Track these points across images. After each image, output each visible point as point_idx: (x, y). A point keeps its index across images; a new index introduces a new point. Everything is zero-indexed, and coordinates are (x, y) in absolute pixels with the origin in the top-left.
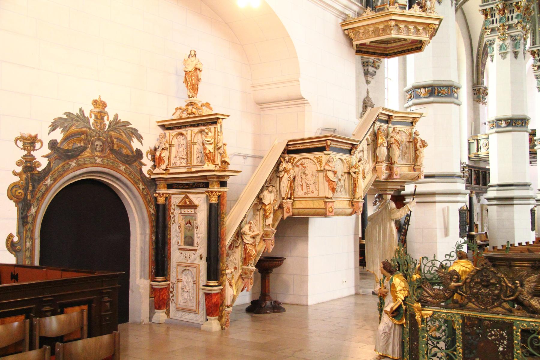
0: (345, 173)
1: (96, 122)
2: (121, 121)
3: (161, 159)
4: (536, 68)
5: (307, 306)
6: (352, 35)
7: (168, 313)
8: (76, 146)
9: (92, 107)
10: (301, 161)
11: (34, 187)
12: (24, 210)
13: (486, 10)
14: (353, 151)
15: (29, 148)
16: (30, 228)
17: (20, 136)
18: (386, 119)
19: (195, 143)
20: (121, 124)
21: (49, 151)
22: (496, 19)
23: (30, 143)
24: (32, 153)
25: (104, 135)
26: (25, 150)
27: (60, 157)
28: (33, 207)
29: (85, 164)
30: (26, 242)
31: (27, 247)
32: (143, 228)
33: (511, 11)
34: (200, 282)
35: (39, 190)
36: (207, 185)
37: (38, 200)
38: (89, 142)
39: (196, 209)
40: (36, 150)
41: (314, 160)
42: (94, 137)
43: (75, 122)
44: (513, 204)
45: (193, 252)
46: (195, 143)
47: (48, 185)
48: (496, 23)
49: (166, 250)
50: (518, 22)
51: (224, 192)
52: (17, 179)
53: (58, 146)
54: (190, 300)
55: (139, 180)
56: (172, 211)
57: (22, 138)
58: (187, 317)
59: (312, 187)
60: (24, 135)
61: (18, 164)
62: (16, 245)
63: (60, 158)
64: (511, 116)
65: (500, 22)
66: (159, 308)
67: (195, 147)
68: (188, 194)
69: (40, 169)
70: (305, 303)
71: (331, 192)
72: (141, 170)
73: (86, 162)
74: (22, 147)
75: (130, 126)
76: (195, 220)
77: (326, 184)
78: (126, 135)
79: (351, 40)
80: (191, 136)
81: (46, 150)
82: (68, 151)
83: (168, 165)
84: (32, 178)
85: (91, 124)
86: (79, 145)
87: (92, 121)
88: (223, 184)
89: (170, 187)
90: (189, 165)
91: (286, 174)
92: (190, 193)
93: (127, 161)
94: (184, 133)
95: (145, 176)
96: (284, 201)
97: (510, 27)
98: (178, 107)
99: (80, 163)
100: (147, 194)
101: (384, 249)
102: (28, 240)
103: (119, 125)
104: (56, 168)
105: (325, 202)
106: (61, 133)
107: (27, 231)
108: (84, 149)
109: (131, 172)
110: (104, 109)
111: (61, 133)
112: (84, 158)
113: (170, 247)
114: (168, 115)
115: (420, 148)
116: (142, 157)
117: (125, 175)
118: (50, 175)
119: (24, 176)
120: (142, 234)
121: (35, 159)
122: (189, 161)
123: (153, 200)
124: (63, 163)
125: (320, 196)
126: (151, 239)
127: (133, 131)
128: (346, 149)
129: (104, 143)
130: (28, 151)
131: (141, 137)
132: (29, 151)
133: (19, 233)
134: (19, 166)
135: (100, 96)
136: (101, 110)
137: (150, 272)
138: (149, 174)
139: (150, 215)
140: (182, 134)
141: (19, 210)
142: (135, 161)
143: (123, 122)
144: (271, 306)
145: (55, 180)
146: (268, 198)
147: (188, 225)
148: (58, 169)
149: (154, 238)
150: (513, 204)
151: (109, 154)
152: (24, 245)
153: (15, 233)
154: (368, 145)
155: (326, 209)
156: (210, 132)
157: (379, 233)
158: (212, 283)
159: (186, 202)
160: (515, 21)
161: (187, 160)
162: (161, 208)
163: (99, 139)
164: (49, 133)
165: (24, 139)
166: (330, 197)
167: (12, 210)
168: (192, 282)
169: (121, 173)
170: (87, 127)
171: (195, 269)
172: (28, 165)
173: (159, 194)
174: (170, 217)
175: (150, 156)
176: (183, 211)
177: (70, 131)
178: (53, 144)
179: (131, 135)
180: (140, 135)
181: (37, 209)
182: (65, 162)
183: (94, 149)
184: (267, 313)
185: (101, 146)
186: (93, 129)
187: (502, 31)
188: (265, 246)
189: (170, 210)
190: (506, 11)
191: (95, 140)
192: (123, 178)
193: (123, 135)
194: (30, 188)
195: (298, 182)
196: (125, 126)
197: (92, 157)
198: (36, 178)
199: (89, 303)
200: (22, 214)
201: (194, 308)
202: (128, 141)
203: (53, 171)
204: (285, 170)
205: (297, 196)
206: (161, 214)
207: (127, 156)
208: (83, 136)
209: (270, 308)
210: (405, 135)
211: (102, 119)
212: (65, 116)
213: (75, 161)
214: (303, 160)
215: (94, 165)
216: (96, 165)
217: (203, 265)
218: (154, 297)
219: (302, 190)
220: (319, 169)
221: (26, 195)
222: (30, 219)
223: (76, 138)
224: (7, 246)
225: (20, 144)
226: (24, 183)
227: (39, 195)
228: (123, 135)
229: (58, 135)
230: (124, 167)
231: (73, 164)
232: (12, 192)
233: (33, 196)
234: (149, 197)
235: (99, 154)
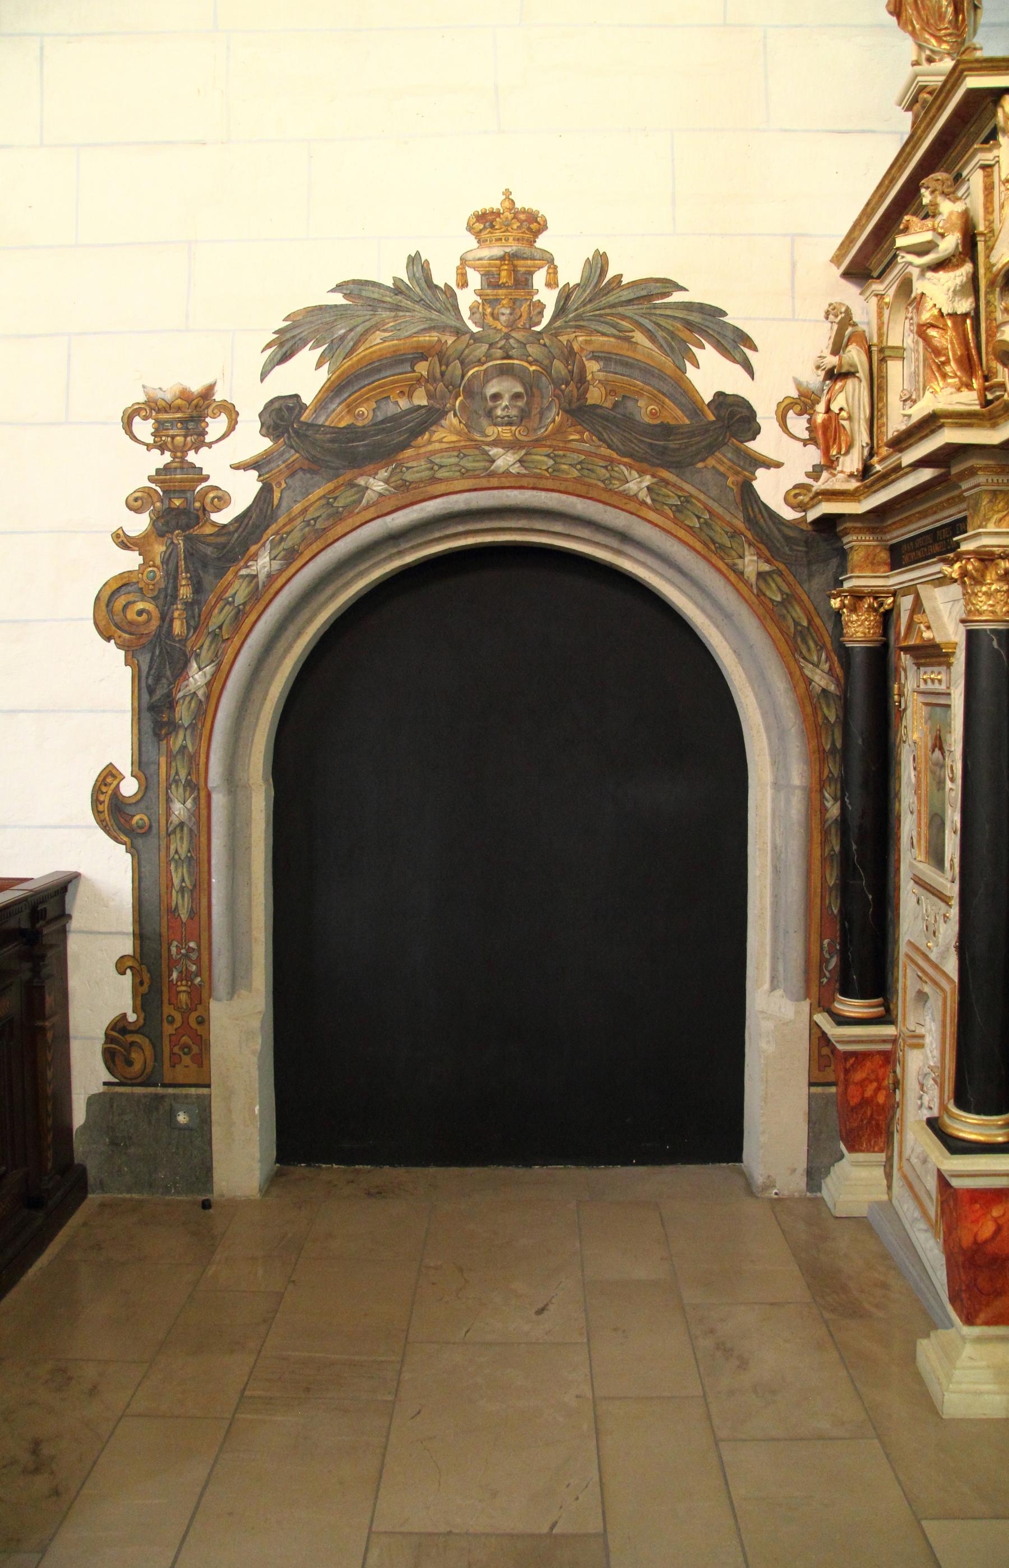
2: (625, 281)
8: (390, 410)
9: (471, 242)
11: (198, 588)
12: (158, 679)
15: (179, 440)
16: (184, 748)
17: (142, 398)
20: (626, 295)
21: (266, 444)
23: (182, 421)
24: (191, 457)
25: (533, 350)
26: (162, 448)
27: (314, 460)
28: (195, 665)
29: (434, 480)
30: (169, 800)
31: (175, 820)
35: (220, 598)
37: (215, 636)
40: (210, 445)
42: (480, 362)
43: (385, 314)
47: (262, 577)
52: (131, 561)
55: (735, 534)
57: (151, 407)
60: (160, 395)
61: (136, 504)
62: (130, 810)
69: (222, 517)
72: (747, 492)
73: (441, 474)
74: (150, 440)
75: (677, 297)
78: (652, 337)
81: (252, 440)
82: (351, 433)
84: (190, 554)
85: (465, 313)
86: (404, 404)
87: (466, 299)
93: (664, 451)
99: (409, 476)
100: (788, 600)
102: (177, 793)
103: (612, 298)
104: (297, 508)
106: (319, 365)
107: (171, 757)
108: (429, 418)
109: (688, 499)
110: (531, 243)
111: (319, 365)
112: (429, 457)
116: (754, 431)
118: (269, 535)
119: (159, 549)
121: (207, 478)
124: (331, 486)
126: (815, 808)
127: (695, 318)
129: (531, 387)
130: (174, 452)
132: (179, 452)
133: (141, 765)
134: (137, 510)
135: (507, 193)
136: (512, 247)
137: (812, 967)
141: (137, 678)
142: (711, 449)
143: (634, 284)
145: (291, 555)
148: (304, 511)
151: (559, 431)
152: (162, 810)
153: (125, 766)
163: (504, 371)
164: (263, 376)
165: (159, 411)
167: (109, 677)
170: (443, 329)
172: (176, 506)
178: (282, 417)
179: (685, 334)
180: (737, 330)
181: (214, 675)
182: (341, 480)
185: (516, 396)
186: (475, 329)
191: (487, 377)
192: (642, 530)
194: (185, 591)
196: (649, 297)
197: (472, 445)
198: (209, 550)
200: (151, 691)
203: (281, 521)
207: (667, 430)
208: (422, 368)
211: (523, 282)
213: (383, 474)
215: (484, 482)
216: (494, 482)
221: (165, 618)
222: (183, 713)
223: (388, 377)
224: (97, 812)
225: (144, 429)
226: (160, 574)
227: (220, 617)
228: (639, 337)
229: (306, 377)
230: (648, 480)
231: (376, 485)
232: (110, 611)
233: (196, 623)
234: (798, 612)
235: (506, 433)
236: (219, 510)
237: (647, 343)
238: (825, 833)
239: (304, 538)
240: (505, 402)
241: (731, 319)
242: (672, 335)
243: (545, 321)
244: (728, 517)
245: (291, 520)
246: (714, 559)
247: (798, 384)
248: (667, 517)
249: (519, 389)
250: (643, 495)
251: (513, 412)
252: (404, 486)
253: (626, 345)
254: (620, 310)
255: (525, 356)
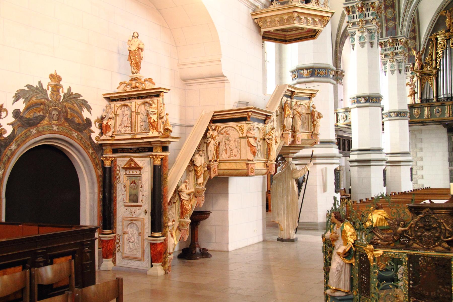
0: (261, 139)
1: (53, 94)
2: (74, 93)
3: (108, 127)
4: (383, 56)
5: (228, 252)
6: (260, 24)
7: (114, 262)
8: (36, 115)
9: (49, 81)
10: (225, 130)
13: (348, 7)
14: (267, 121)
18: (290, 94)
19: (138, 113)
20: (74, 96)
22: (356, 15)
25: (60, 105)
29: (44, 131)
32: (92, 188)
33: (367, 9)
34: (145, 233)
35: (5, 154)
36: (151, 150)
37: (4, 163)
38: (47, 111)
39: (140, 170)
40: (2, 118)
41: (237, 128)
43: (35, 94)
44: (370, 166)
45: (138, 208)
46: (138, 113)
47: (13, 150)
48: (356, 18)
49: (112, 206)
50: (373, 19)
51: (166, 156)
53: (21, 115)
54: (136, 249)
56: (118, 172)
58: (132, 264)
59: (235, 151)
63: (23, 126)
64: (368, 94)
65: (359, 17)
66: (107, 257)
67: (139, 116)
68: (133, 158)
69: (5, 136)
70: (226, 249)
71: (252, 155)
75: (81, 98)
76: (140, 180)
77: (248, 148)
78: (77, 105)
79: (259, 28)
80: (135, 107)
82: (29, 119)
83: (114, 132)
85: (49, 96)
86: (39, 114)
87: (49, 93)
88: (165, 149)
89: (115, 151)
90: (133, 132)
91: (212, 140)
92: (134, 157)
93: (78, 129)
94: (129, 104)
95: (94, 142)
96: (211, 163)
97: (367, 22)
98: (123, 81)
100: (96, 157)
101: (287, 203)
103: (71, 97)
104: (20, 135)
105: (247, 164)
106: (24, 103)
108: (43, 118)
109: (82, 138)
110: (59, 83)
111: (24, 103)
113: (116, 204)
114: (113, 88)
115: (317, 119)
117: (77, 141)
118: (14, 141)
120: (90, 193)
121: (2, 126)
122: (133, 129)
123: (100, 163)
124: (26, 130)
125: (242, 159)
126: (99, 197)
127: (84, 102)
128: (262, 119)
129: (59, 112)
131: (90, 108)
135: (56, 71)
136: (56, 83)
138: (97, 140)
139: (98, 176)
140: (126, 105)
142: (85, 129)
144: (200, 253)
145: (19, 146)
146: (200, 161)
147: (133, 184)
148: (21, 136)
149: (101, 196)
150: (370, 166)
151: (63, 123)
154: (277, 116)
155: (248, 169)
156: (154, 103)
157: (283, 190)
158: (157, 234)
159: (131, 164)
160: (371, 17)
161: (132, 128)
162: (107, 171)
163: (55, 109)
164: (13, 104)
166: (251, 159)
168: (137, 234)
169: (74, 139)
171: (140, 223)
173: (106, 157)
174: (116, 178)
175: (97, 125)
176: (128, 172)
177: (31, 101)
178: (16, 113)
179: (82, 105)
181: (4, 172)
182: (28, 129)
183: (51, 118)
184: (197, 259)
185: (57, 115)
186: (51, 100)
187: (361, 25)
188: (196, 202)
189: (115, 171)
190: (364, 9)
192: (76, 144)
193: (76, 105)
195: (222, 147)
196: (77, 97)
197: (50, 125)
198: (3, 143)
199: (72, 254)
201: (140, 256)
202: (79, 110)
203: (17, 137)
204: (212, 137)
205: (222, 159)
206: (107, 175)
207: (79, 124)
208: (42, 107)
209: (199, 255)
210: (304, 108)
211: (58, 91)
212: (26, 88)
213: (35, 129)
214: (227, 128)
215: (52, 132)
216: (53, 132)
217: (147, 220)
218: (102, 248)
219: (226, 154)
220: (241, 136)
223: (36, 108)
228: (76, 105)
229: (21, 105)
230: (76, 134)
231: (34, 131)
234: (97, 160)
236: (4, 134)
238: (100, 201)
239: (21, 142)
240: (55, 116)
241: (88, 103)
243: (62, 100)
245: (19, 138)
247: (97, 117)
249: (57, 113)
251: (56, 118)
252: (39, 132)
255: (58, 107)
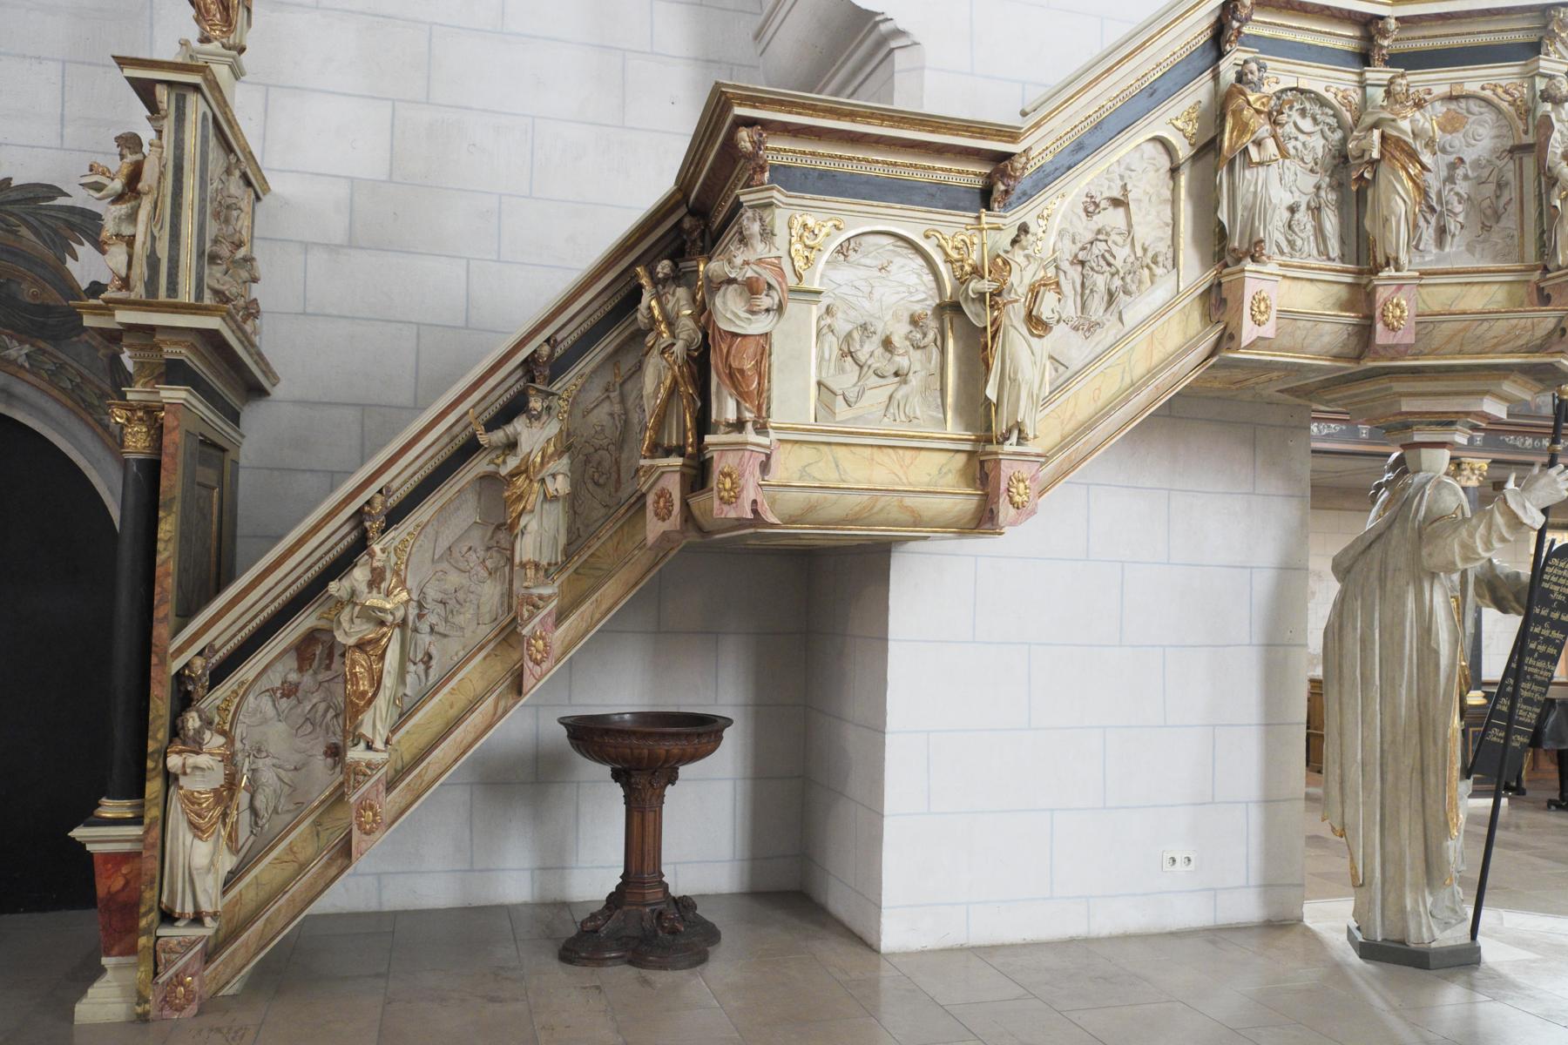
2: (14, 183)
20: (14, 196)
75: (60, 201)
78: (36, 232)
109: (62, 366)
127: (76, 219)
179: (68, 233)
196: (36, 199)
207: (47, 310)
210: (1489, 116)
228: (24, 231)
230: (26, 349)
237: (33, 237)
242: (56, 232)
244: (96, 380)
246: (83, 414)
248: (42, 379)
250: (22, 360)
253: (12, 237)
254: (9, 207)
